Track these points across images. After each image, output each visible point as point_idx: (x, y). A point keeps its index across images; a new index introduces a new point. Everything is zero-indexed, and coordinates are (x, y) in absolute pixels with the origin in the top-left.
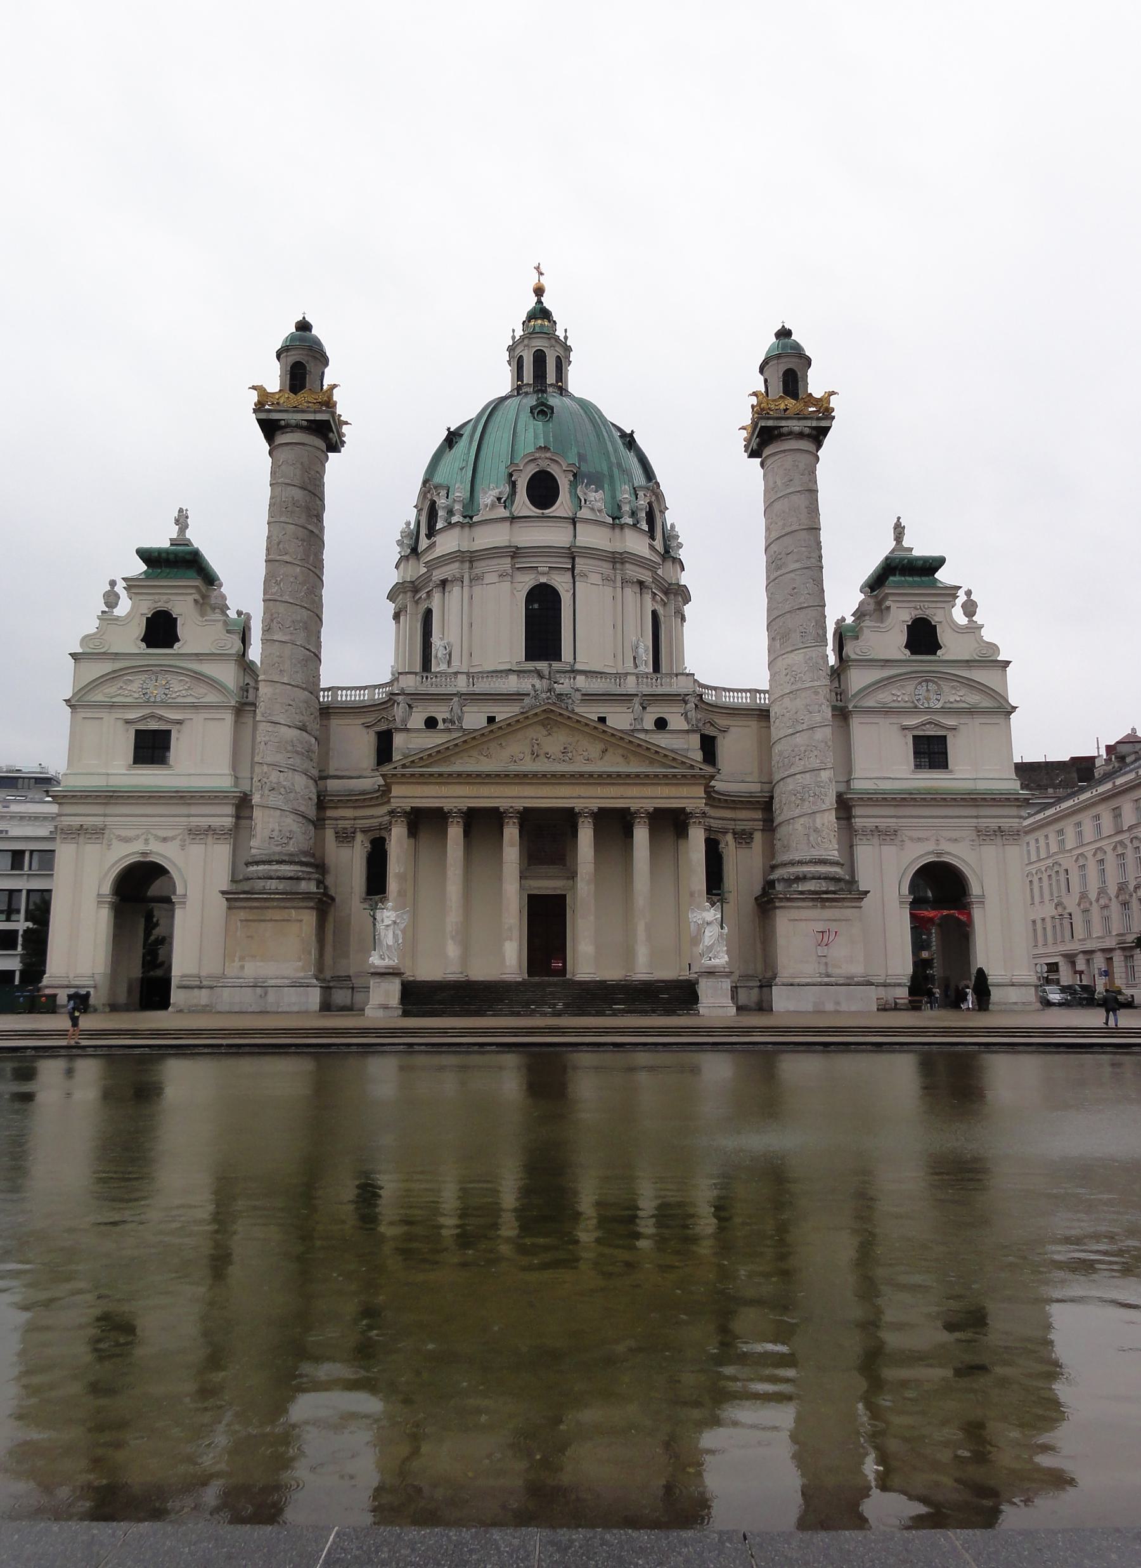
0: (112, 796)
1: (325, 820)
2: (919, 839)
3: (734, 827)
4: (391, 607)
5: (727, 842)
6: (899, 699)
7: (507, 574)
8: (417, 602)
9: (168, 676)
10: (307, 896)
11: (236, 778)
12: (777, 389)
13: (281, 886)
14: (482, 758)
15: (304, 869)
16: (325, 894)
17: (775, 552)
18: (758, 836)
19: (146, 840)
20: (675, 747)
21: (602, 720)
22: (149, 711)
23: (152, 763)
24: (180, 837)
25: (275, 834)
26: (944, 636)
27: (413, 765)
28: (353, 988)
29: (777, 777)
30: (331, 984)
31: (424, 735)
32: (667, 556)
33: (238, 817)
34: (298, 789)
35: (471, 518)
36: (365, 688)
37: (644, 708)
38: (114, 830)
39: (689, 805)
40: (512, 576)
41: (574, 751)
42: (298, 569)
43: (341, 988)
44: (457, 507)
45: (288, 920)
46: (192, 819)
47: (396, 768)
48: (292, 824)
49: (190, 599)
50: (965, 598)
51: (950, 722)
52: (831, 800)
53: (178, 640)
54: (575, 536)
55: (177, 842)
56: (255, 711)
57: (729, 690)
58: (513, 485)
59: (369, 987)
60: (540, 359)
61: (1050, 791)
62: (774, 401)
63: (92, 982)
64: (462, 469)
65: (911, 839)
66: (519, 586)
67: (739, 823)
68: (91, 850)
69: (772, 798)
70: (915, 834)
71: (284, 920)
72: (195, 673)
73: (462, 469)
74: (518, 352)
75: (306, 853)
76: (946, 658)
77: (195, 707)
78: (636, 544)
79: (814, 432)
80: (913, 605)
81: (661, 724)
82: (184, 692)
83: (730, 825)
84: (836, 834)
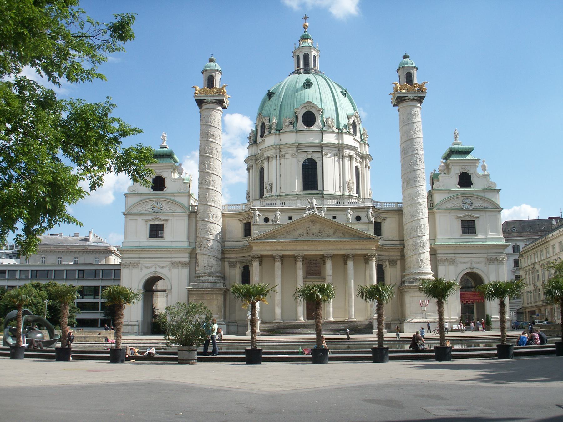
0: (142, 251)
1: (224, 258)
2: (464, 263)
3: (388, 259)
4: (245, 166)
6: (456, 206)
7: (295, 155)
8: (257, 164)
9: (162, 202)
10: (220, 289)
11: (189, 242)
12: (404, 79)
13: (209, 285)
14: (287, 235)
15: (217, 278)
16: (226, 289)
17: (404, 147)
18: (399, 263)
19: (155, 267)
20: (364, 229)
21: (334, 218)
22: (155, 216)
23: (157, 237)
24: (168, 266)
25: (206, 265)
26: (474, 179)
27: (261, 238)
28: (237, 325)
29: (406, 239)
30: (229, 324)
31: (265, 226)
32: (362, 142)
33: (190, 258)
34: (214, 247)
35: (279, 131)
36: (239, 205)
37: (350, 214)
38: (143, 264)
40: (297, 155)
41: (324, 232)
42: (212, 159)
43: (233, 325)
44: (274, 126)
45: (213, 299)
46: (173, 259)
47: (254, 240)
48: (213, 261)
50: (482, 163)
52: (427, 249)
54: (322, 138)
55: (167, 268)
56: (196, 215)
57: (386, 203)
58: (297, 117)
59: (248, 325)
60: (306, 57)
61: (539, 233)
62: (403, 86)
63: (137, 324)
64: (275, 109)
65: (461, 263)
66: (300, 159)
67: (390, 257)
68: (135, 272)
69: (404, 247)
70: (463, 261)
71: (211, 299)
72: (172, 201)
73: (275, 109)
74: (297, 54)
75: (218, 272)
77: (173, 214)
78: (348, 140)
79: (419, 98)
80: (460, 167)
81: (358, 218)
82: (168, 208)
83: (388, 258)
84: (430, 261)
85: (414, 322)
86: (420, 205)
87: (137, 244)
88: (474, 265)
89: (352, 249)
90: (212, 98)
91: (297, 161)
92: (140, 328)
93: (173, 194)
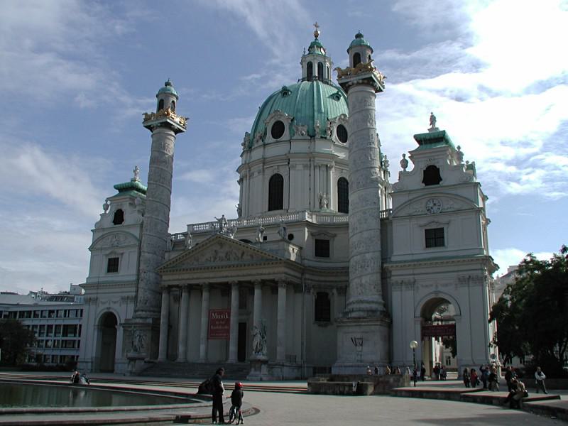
2: (427, 286)
5: (333, 294)
10: (148, 325)
15: (152, 313)
19: (110, 304)
39: (276, 277)
49: (128, 203)
51: (444, 219)
53: (123, 220)
58: (266, 129)
60: (310, 66)
65: (422, 286)
66: (266, 176)
68: (93, 307)
76: (444, 185)
77: (126, 247)
79: (366, 81)
85: (345, 367)
86: (365, 213)
87: (96, 280)
88: (440, 288)
89: (258, 274)
90: (157, 122)
91: (264, 179)
92: (94, 365)
93: (128, 226)
